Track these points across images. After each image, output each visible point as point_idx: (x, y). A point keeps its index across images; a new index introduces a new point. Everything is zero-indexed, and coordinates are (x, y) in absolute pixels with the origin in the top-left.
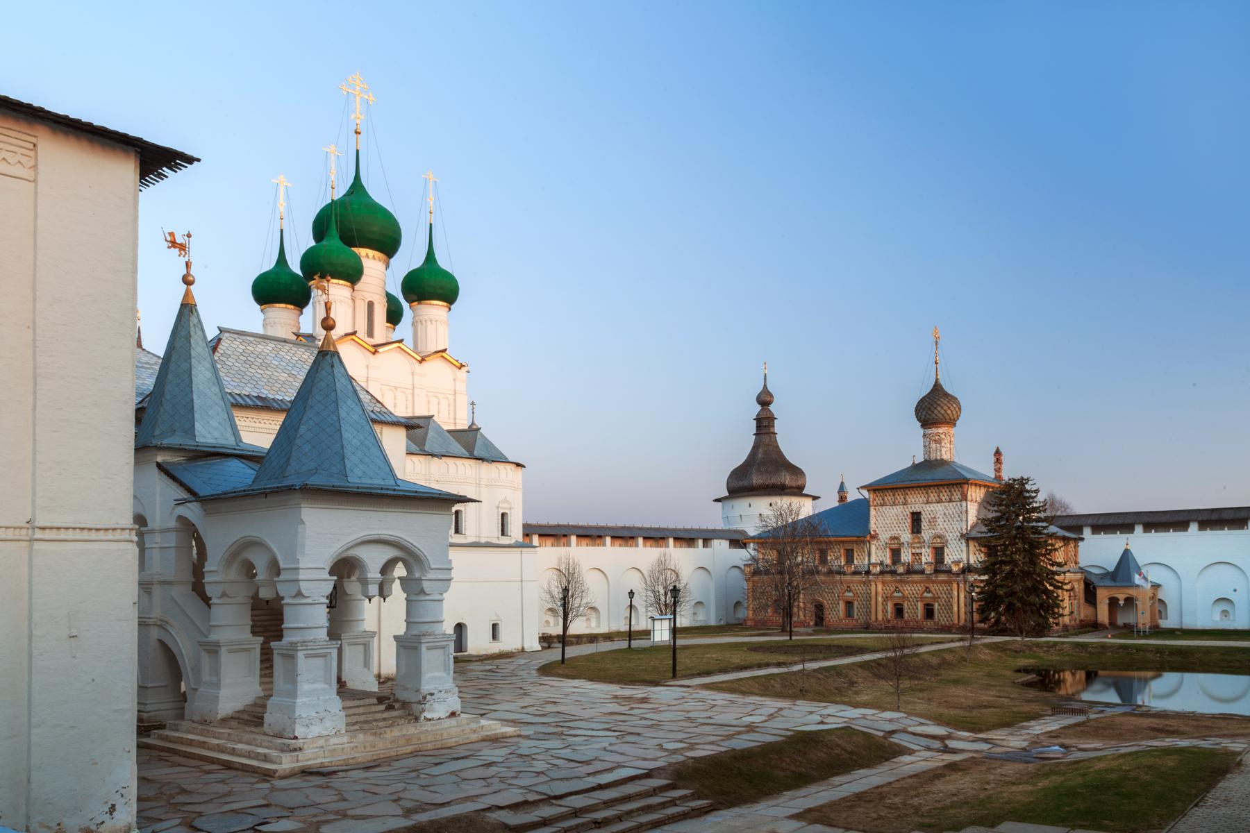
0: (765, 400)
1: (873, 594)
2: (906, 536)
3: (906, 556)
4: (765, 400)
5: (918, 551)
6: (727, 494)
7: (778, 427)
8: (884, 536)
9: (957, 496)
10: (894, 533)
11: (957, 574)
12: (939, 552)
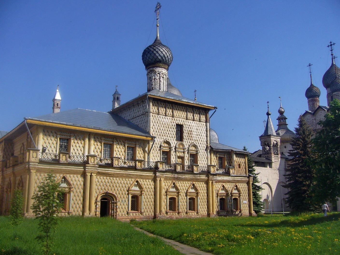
2: (174, 142)
5: (182, 154)
8: (159, 141)
12: (194, 157)
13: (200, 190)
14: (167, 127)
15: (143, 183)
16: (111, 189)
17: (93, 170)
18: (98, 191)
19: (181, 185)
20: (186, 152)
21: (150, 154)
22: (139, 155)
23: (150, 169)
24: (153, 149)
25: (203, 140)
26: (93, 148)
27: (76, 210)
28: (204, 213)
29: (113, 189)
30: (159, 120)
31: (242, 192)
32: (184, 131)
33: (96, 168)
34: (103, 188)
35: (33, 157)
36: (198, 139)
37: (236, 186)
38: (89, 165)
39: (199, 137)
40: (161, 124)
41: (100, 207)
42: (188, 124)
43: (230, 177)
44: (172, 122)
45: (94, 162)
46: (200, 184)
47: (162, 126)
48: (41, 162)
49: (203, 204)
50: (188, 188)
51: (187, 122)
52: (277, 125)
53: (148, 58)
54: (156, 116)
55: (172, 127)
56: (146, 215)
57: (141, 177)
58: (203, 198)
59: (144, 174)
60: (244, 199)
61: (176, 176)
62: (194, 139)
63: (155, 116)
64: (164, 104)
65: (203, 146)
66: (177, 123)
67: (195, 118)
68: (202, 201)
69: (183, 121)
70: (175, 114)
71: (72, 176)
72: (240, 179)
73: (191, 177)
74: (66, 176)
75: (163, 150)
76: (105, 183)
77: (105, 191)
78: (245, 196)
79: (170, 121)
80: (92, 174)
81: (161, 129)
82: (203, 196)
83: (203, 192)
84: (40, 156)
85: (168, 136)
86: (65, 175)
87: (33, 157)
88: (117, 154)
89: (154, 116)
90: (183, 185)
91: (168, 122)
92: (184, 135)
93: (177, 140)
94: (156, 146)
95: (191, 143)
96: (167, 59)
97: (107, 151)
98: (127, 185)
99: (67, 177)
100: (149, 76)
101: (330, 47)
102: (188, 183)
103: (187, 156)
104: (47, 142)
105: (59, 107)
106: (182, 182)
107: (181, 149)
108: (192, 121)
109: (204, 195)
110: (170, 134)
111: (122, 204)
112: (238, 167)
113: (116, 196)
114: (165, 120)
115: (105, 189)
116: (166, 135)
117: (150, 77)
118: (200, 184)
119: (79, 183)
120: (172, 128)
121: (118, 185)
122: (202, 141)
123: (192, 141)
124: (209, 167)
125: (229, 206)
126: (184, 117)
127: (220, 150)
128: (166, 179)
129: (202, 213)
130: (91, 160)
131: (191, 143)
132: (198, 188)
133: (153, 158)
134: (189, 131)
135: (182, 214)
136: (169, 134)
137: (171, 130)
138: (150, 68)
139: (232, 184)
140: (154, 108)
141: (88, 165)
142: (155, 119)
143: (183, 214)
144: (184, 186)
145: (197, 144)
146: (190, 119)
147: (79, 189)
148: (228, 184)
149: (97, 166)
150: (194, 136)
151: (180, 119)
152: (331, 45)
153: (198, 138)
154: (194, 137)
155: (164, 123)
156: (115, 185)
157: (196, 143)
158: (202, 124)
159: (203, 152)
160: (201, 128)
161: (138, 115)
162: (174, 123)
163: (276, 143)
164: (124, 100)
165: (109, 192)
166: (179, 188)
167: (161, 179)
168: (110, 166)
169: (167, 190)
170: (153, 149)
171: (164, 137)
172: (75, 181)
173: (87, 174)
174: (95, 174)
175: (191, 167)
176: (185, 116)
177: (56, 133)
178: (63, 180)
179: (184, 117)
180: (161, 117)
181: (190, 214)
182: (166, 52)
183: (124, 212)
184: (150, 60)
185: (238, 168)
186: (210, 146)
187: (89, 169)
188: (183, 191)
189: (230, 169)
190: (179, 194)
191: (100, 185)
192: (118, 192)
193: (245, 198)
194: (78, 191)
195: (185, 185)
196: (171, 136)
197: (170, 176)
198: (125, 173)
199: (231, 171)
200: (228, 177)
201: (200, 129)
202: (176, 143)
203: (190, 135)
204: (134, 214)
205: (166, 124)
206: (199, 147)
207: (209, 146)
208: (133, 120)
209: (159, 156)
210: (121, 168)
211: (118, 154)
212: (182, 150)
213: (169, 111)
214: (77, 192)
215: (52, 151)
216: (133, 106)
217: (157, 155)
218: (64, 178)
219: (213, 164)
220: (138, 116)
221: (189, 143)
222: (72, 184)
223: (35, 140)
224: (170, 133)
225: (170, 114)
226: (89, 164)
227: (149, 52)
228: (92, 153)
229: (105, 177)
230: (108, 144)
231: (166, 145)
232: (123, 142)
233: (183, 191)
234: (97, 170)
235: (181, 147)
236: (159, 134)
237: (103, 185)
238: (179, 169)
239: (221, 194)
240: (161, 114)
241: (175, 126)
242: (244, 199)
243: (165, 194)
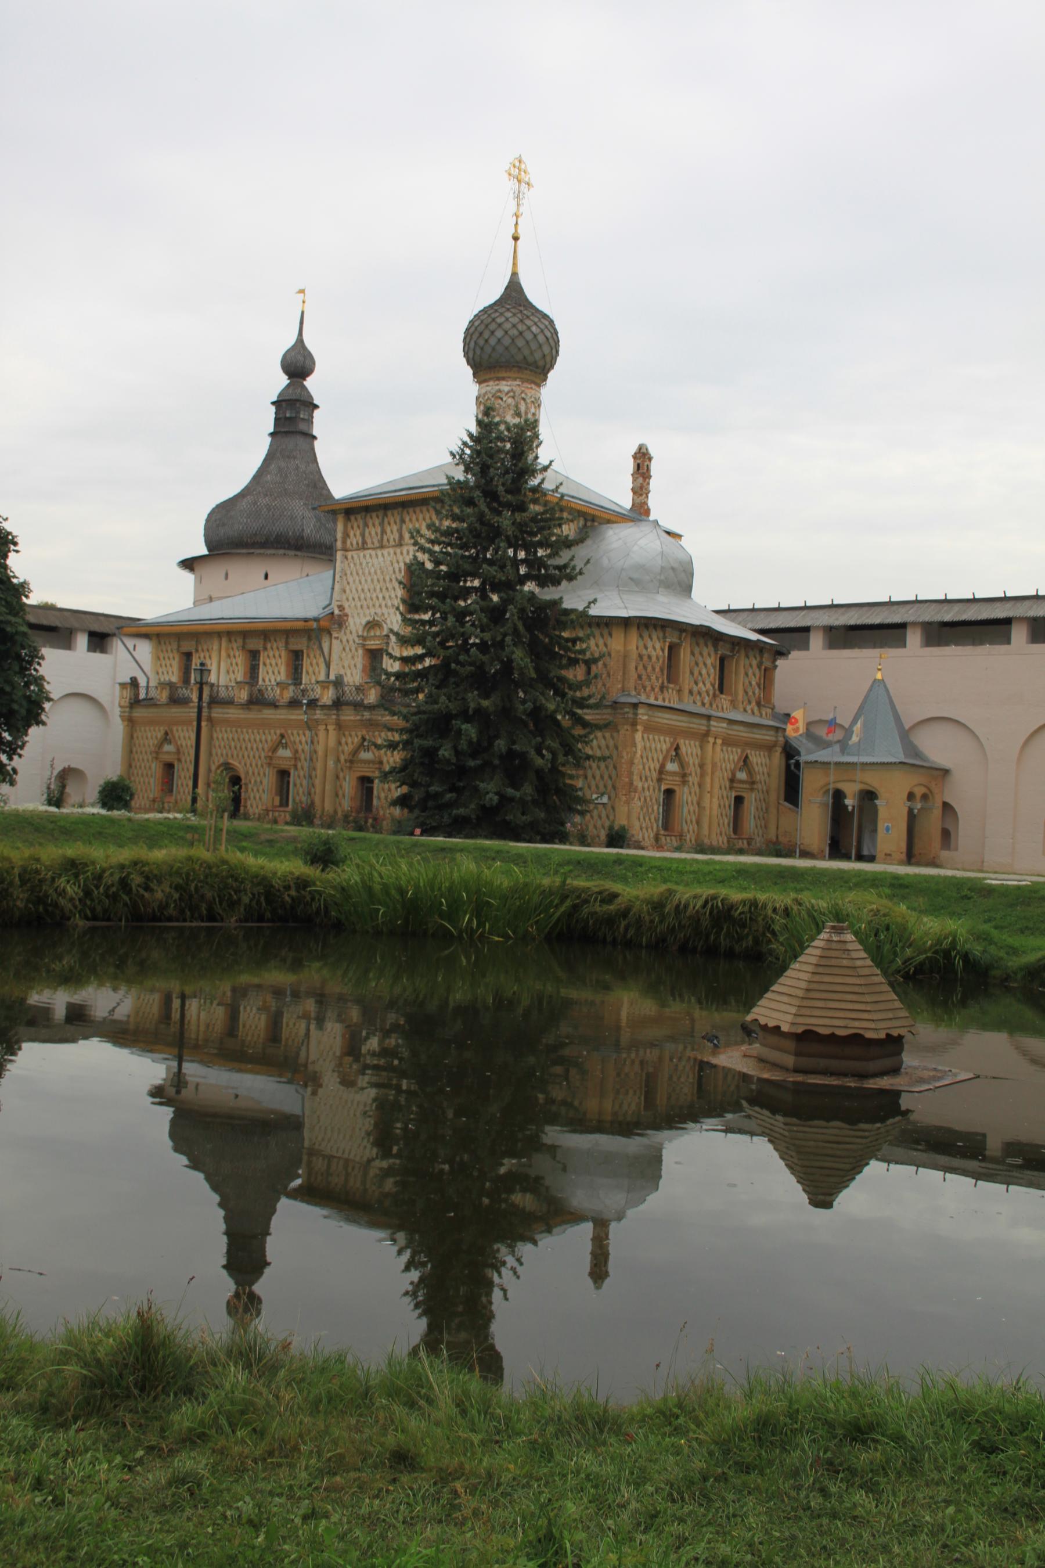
0: (298, 365)
4: (298, 365)
6: (203, 551)
7: (321, 424)
8: (356, 623)
24: (344, 649)
30: (361, 564)
54: (356, 557)
59: (293, 717)
60: (597, 786)
61: (367, 715)
63: (352, 557)
78: (602, 777)
79: (388, 559)
81: (366, 588)
89: (349, 557)
91: (382, 564)
111: (255, 789)
114: (375, 560)
116: (377, 605)
136: (384, 598)
142: (352, 565)
155: (372, 570)
162: (398, 562)
170: (344, 649)
197: (352, 718)
204: (277, 814)
205: (379, 572)
213: (392, 532)
241: (400, 571)
242: (597, 786)
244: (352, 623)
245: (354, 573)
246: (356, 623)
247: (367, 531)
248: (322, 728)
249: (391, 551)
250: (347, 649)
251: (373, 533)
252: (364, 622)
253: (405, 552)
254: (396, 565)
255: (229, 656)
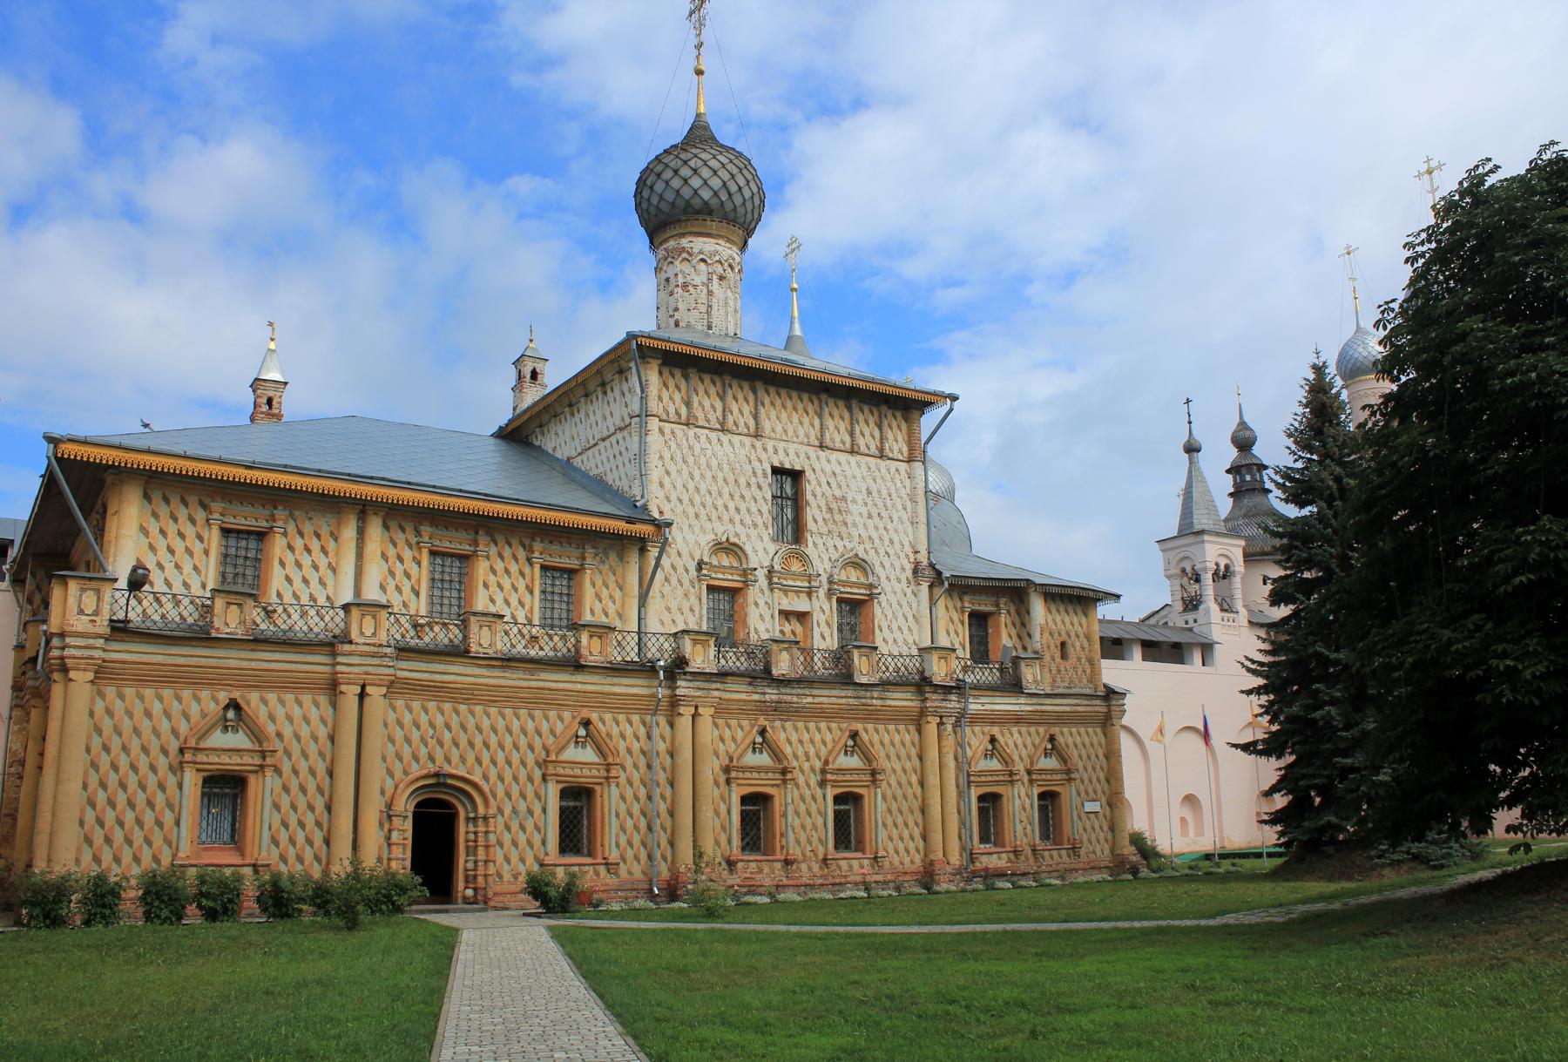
1: (687, 754)
2: (762, 550)
3: (761, 622)
5: (801, 605)
9: (896, 442)
10: (723, 530)
11: (947, 690)
13: (888, 756)
14: (731, 479)
15: (615, 731)
16: (463, 759)
17: (370, 669)
18: (398, 768)
19: (794, 738)
20: (822, 592)
21: (650, 600)
22: (598, 607)
23: (647, 669)
24: (667, 579)
25: (896, 540)
26: (375, 572)
27: (291, 852)
28: (907, 860)
29: (471, 758)
31: (1080, 765)
32: (809, 497)
33: (386, 661)
34: (423, 751)
35: (81, 612)
36: (875, 535)
37: (1052, 739)
38: (353, 647)
39: (881, 526)
40: (704, 466)
41: (409, 842)
42: (828, 468)
43: (1022, 700)
44: (753, 457)
45: (374, 634)
46: (887, 731)
47: (709, 475)
48: (120, 629)
49: (900, 820)
50: (830, 752)
51: (824, 461)
52: (1231, 495)
53: (655, 200)
54: (679, 434)
55: (753, 480)
56: (630, 873)
57: (605, 702)
58: (899, 792)
59: (617, 689)
61: (772, 694)
62: (855, 533)
64: (717, 379)
65: (897, 564)
66: (777, 464)
67: (861, 442)
68: (894, 807)
69: (802, 456)
70: (767, 426)
71: (272, 697)
72: (1068, 709)
73: (843, 701)
74: (242, 697)
75: (712, 582)
76: (431, 732)
77: (430, 765)
80: (369, 689)
81: (703, 487)
82: (899, 784)
83: (898, 767)
84: (116, 602)
85: (737, 518)
86: (236, 694)
87: (81, 612)
88: (492, 601)
89: (667, 431)
90: (806, 737)
91: (732, 457)
92: (809, 518)
93: (775, 540)
94: (679, 564)
95: (841, 549)
96: (738, 200)
97: (446, 586)
98: (537, 738)
99: (249, 704)
100: (663, 276)
101: (1426, 177)
102: (829, 729)
103: (826, 607)
104: (161, 544)
105: (274, 415)
106: (800, 725)
107: (794, 575)
108: (843, 457)
109: (904, 780)
110: (743, 510)
111: (515, 825)
112: (1058, 655)
113: (486, 787)
115: (432, 758)
116: (726, 518)
117: (667, 280)
118: (887, 731)
119: (305, 731)
120: (754, 487)
121: (493, 740)
122: (892, 542)
123: (846, 542)
124: (926, 656)
125: (1019, 828)
126: (807, 436)
127: (977, 583)
128: (722, 710)
129: (896, 861)
130: (363, 629)
131: (841, 549)
132: (878, 751)
133: (667, 618)
134: (830, 498)
135: (804, 867)
136: (738, 510)
137: (748, 495)
138: (666, 241)
139: (1032, 729)
140: (671, 398)
141: (347, 647)
142: (674, 446)
143: (810, 869)
144: (812, 741)
145: (871, 557)
146: (838, 445)
147: (305, 756)
148: (1014, 730)
149: (388, 650)
150: (858, 519)
151: (792, 448)
152: (1430, 172)
153: (876, 528)
154: (855, 525)
155: (714, 463)
156: (478, 741)
157: (866, 552)
158: (893, 471)
159: (899, 593)
160: (889, 484)
161: (606, 433)
163: (1227, 567)
164: (555, 376)
165: (448, 769)
166: (788, 750)
167: (701, 710)
168: (459, 652)
169: (731, 760)
170: (667, 579)
171: (717, 524)
172: (290, 719)
173: (343, 688)
174: (384, 690)
175: (841, 658)
176: (813, 434)
177: (205, 507)
178: (231, 714)
179: (807, 436)
180: (703, 439)
181: (839, 867)
182: (735, 171)
183: (523, 860)
184: (663, 206)
185: (1058, 660)
186: (932, 566)
187: (351, 666)
188: (806, 766)
189: (1023, 664)
190: (789, 776)
191: (406, 743)
192: (493, 773)
193: (1090, 789)
194: (303, 766)
195: (818, 737)
196: (748, 521)
197: (743, 696)
198: (525, 684)
199: (1029, 674)
200: (1013, 700)
201: (884, 493)
202: (772, 552)
203: (838, 517)
205: (726, 468)
206: (878, 569)
207: (925, 562)
208: (584, 457)
209: (692, 610)
210: (507, 661)
211: (499, 599)
212: (798, 583)
214: (296, 772)
215: (185, 584)
216: (586, 396)
217: (686, 605)
218: (234, 705)
219: (944, 641)
220: (603, 440)
221: (832, 550)
222: (273, 734)
223: (100, 531)
224: (743, 507)
225: (741, 424)
226: (351, 642)
227: (659, 175)
228: (372, 593)
229: (432, 705)
230: (452, 555)
231: (725, 561)
232: (524, 546)
233: (806, 766)
234: (391, 671)
235: (796, 567)
236: (691, 511)
237: (424, 741)
238: (783, 665)
239: (981, 773)
240: (700, 423)
243: (722, 778)
244: (679, 540)
245: (679, 459)
246: (689, 541)
247: (695, 399)
248: (687, 711)
249: (748, 441)
250: (674, 581)
251: (707, 403)
252: (706, 539)
253: (770, 450)
254: (756, 464)
255: (384, 556)
